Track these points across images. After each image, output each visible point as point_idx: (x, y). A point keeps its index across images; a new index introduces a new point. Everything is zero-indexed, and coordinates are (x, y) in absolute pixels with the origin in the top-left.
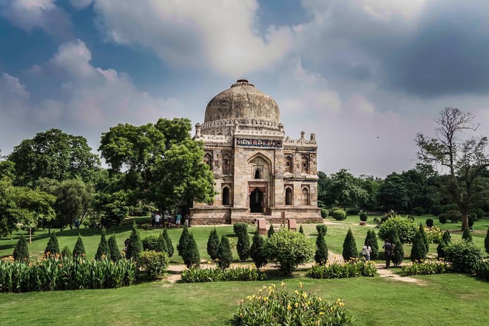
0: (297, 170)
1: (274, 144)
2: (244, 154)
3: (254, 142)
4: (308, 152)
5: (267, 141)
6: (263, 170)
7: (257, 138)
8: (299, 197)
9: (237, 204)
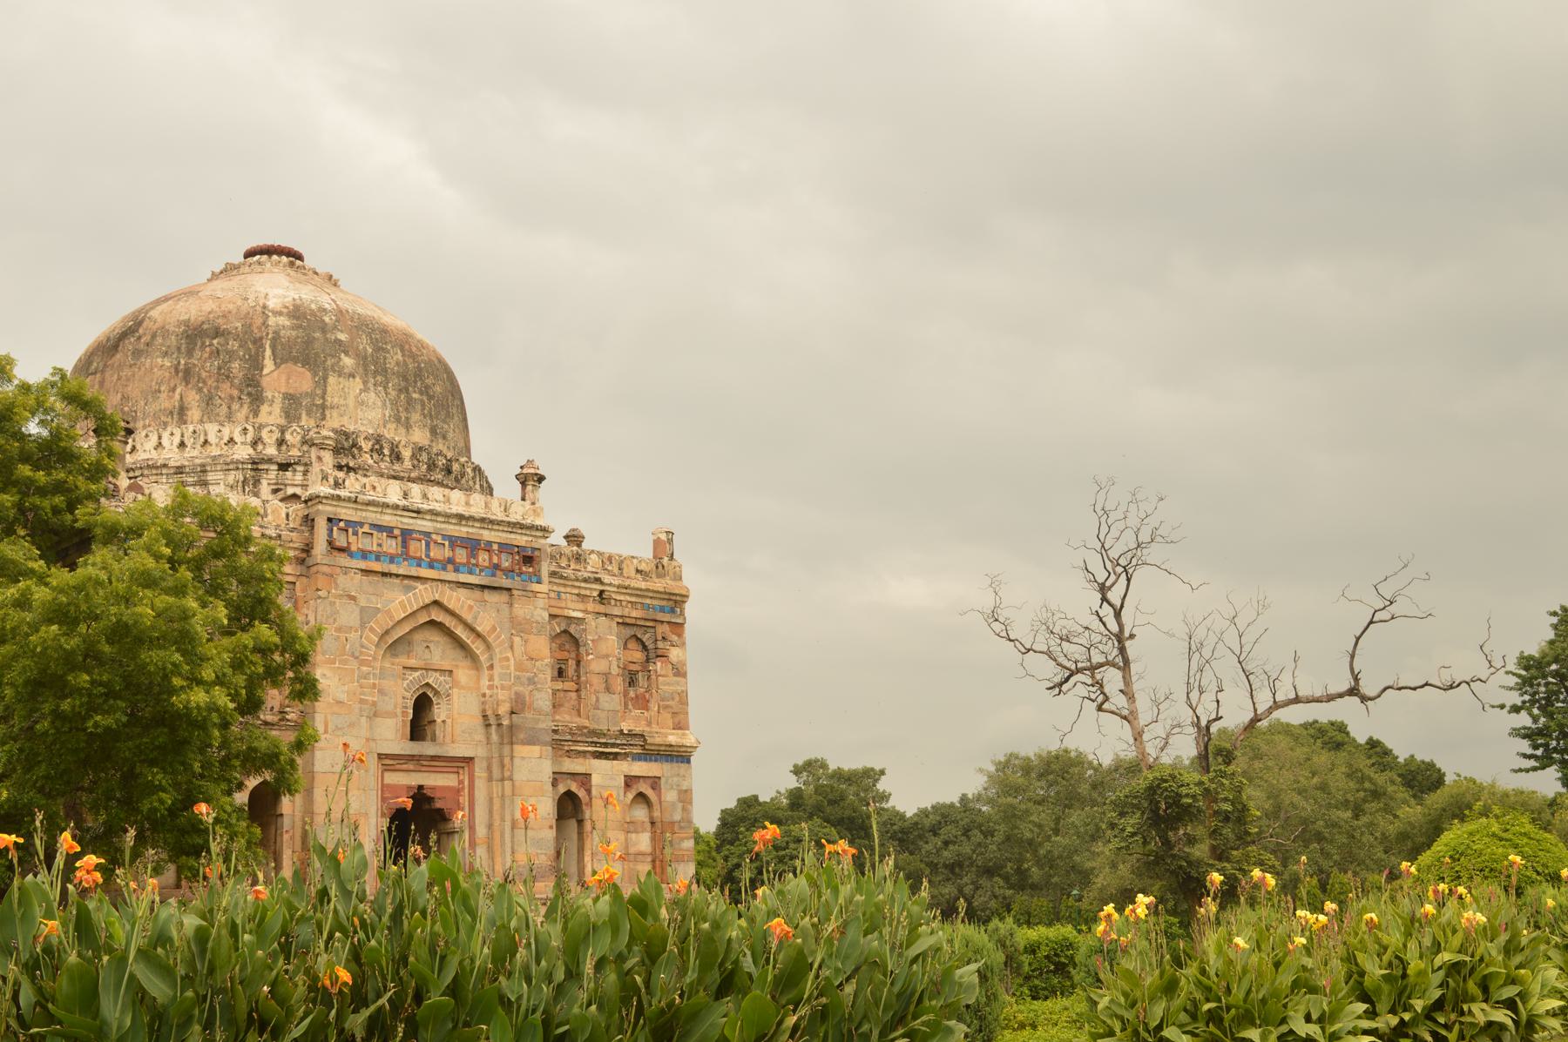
1: (506, 564)
2: (363, 603)
3: (413, 545)
5: (473, 545)
7: (424, 525)
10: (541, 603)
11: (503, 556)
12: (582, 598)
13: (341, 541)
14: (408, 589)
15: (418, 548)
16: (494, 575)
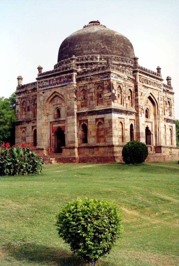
4: (102, 80)
6: (61, 109)
8: (94, 134)
9: (39, 145)
11: (66, 78)
13: (41, 85)
14: (51, 90)
16: (64, 83)
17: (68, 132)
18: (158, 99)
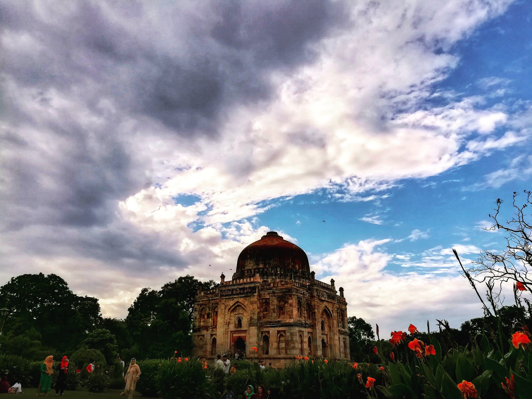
0: (275, 315)
5: (244, 289)
7: (235, 287)
8: (275, 345)
10: (256, 297)
12: (269, 294)
15: (234, 292)
17: (250, 343)
18: (333, 311)
